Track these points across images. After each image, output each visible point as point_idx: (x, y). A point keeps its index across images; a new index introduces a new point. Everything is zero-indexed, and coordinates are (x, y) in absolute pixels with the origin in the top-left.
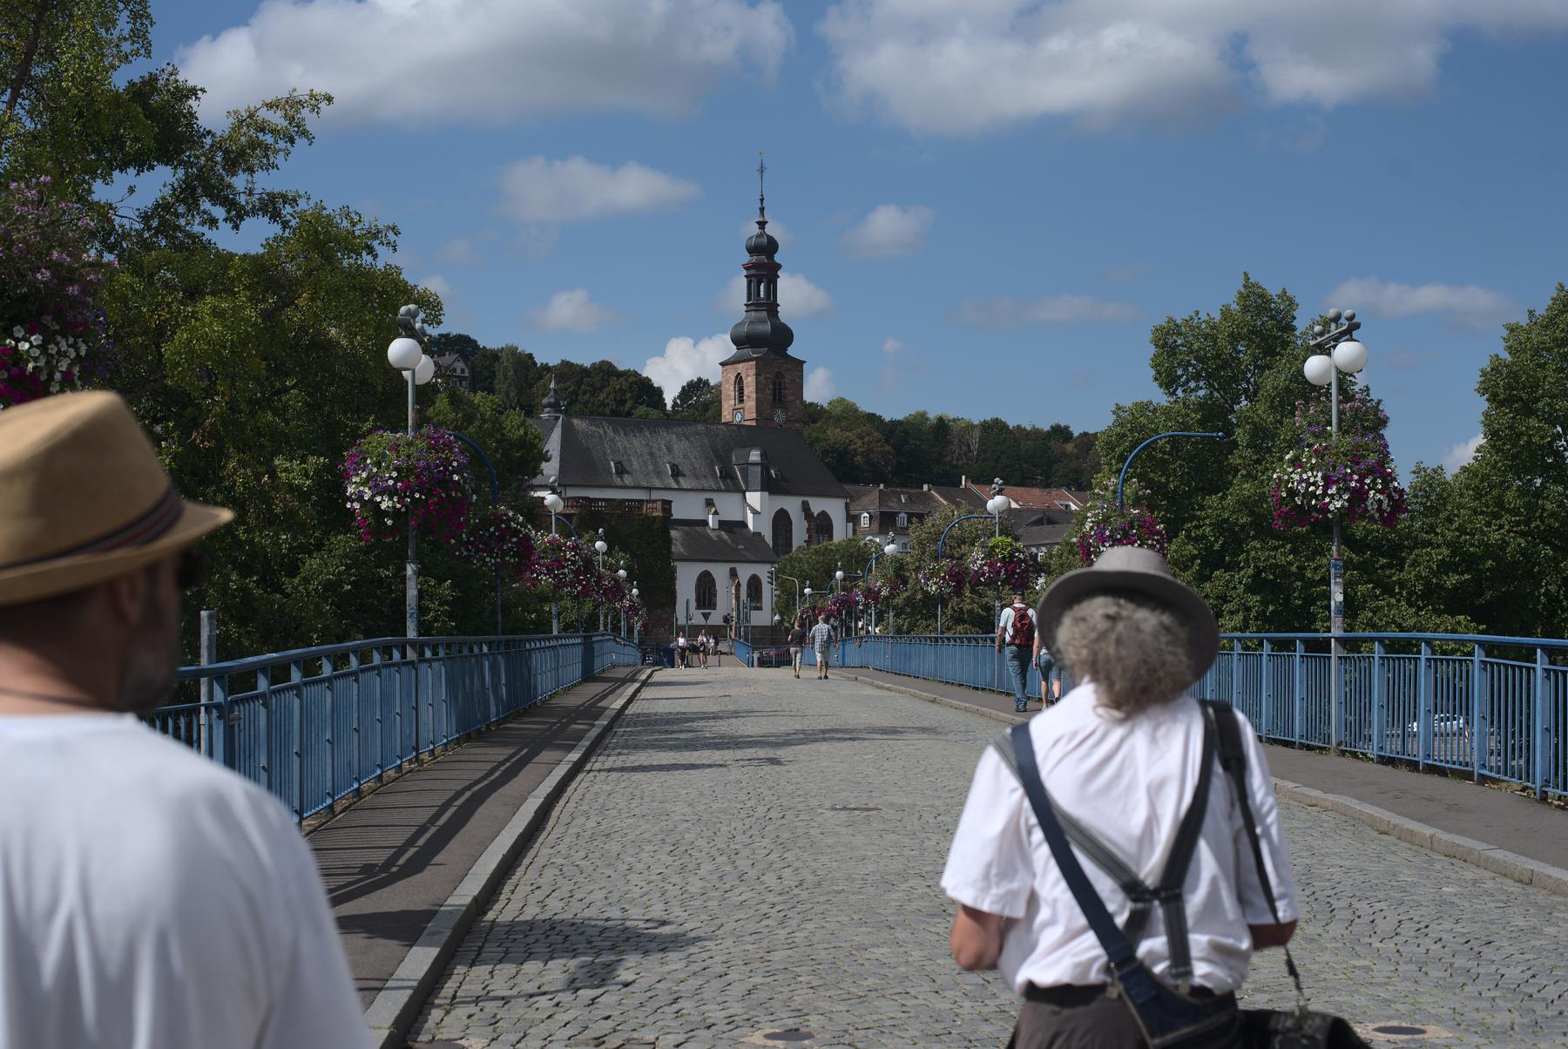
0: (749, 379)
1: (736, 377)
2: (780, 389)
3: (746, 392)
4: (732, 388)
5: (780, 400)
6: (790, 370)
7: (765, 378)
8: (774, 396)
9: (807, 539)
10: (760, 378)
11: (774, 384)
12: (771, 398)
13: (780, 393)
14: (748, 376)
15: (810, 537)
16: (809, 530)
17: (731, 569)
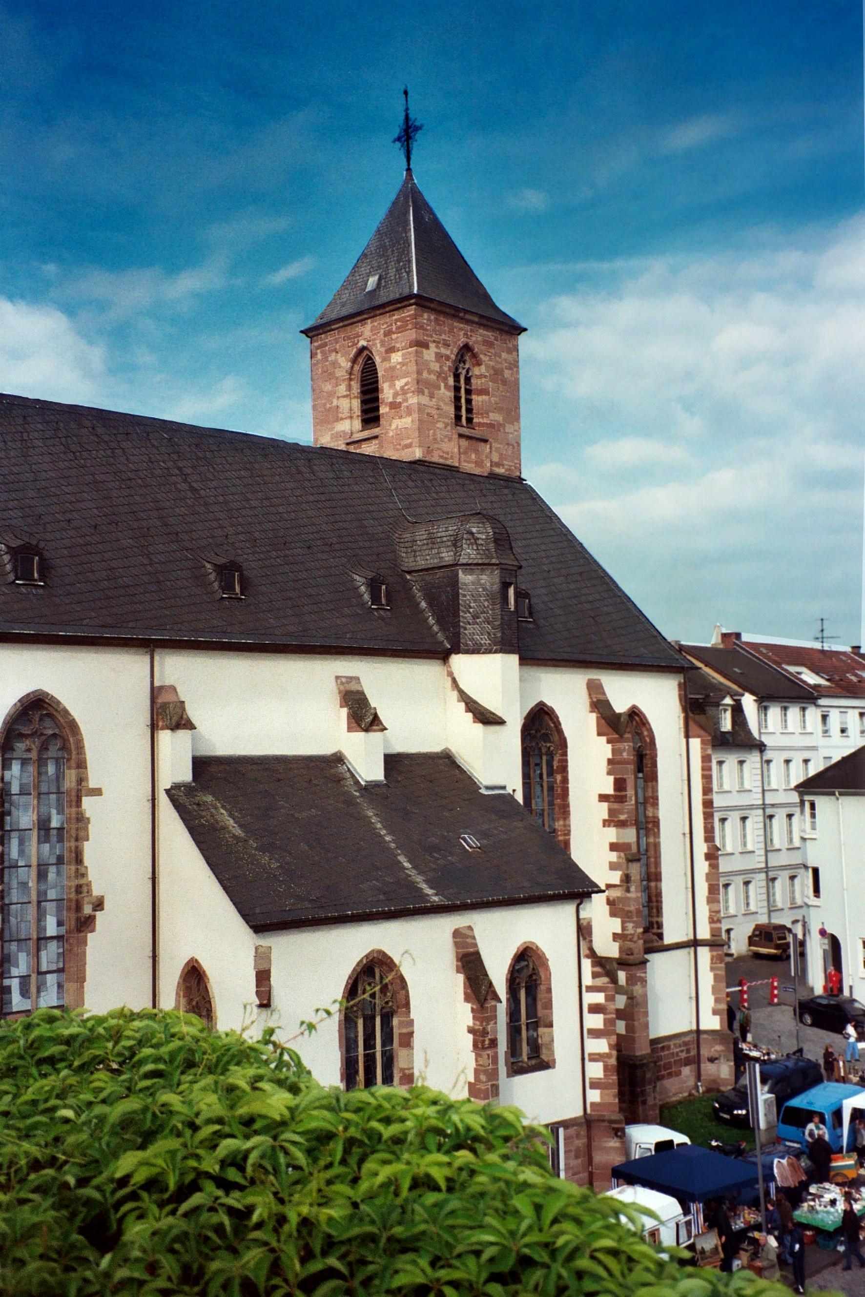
0: (396, 358)
1: (354, 361)
2: (468, 392)
3: (387, 393)
4: (342, 389)
5: (469, 420)
6: (490, 344)
7: (439, 356)
8: (458, 408)
9: (610, 790)
10: (429, 355)
11: (457, 377)
12: (451, 410)
13: (469, 401)
14: (391, 350)
15: (620, 785)
16: (613, 763)
17: (457, 933)
